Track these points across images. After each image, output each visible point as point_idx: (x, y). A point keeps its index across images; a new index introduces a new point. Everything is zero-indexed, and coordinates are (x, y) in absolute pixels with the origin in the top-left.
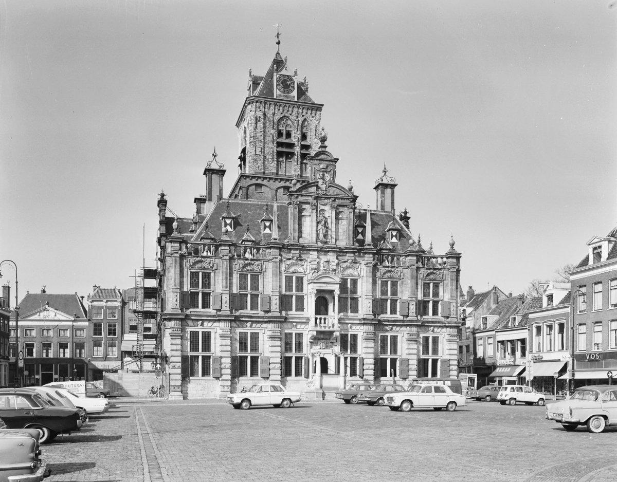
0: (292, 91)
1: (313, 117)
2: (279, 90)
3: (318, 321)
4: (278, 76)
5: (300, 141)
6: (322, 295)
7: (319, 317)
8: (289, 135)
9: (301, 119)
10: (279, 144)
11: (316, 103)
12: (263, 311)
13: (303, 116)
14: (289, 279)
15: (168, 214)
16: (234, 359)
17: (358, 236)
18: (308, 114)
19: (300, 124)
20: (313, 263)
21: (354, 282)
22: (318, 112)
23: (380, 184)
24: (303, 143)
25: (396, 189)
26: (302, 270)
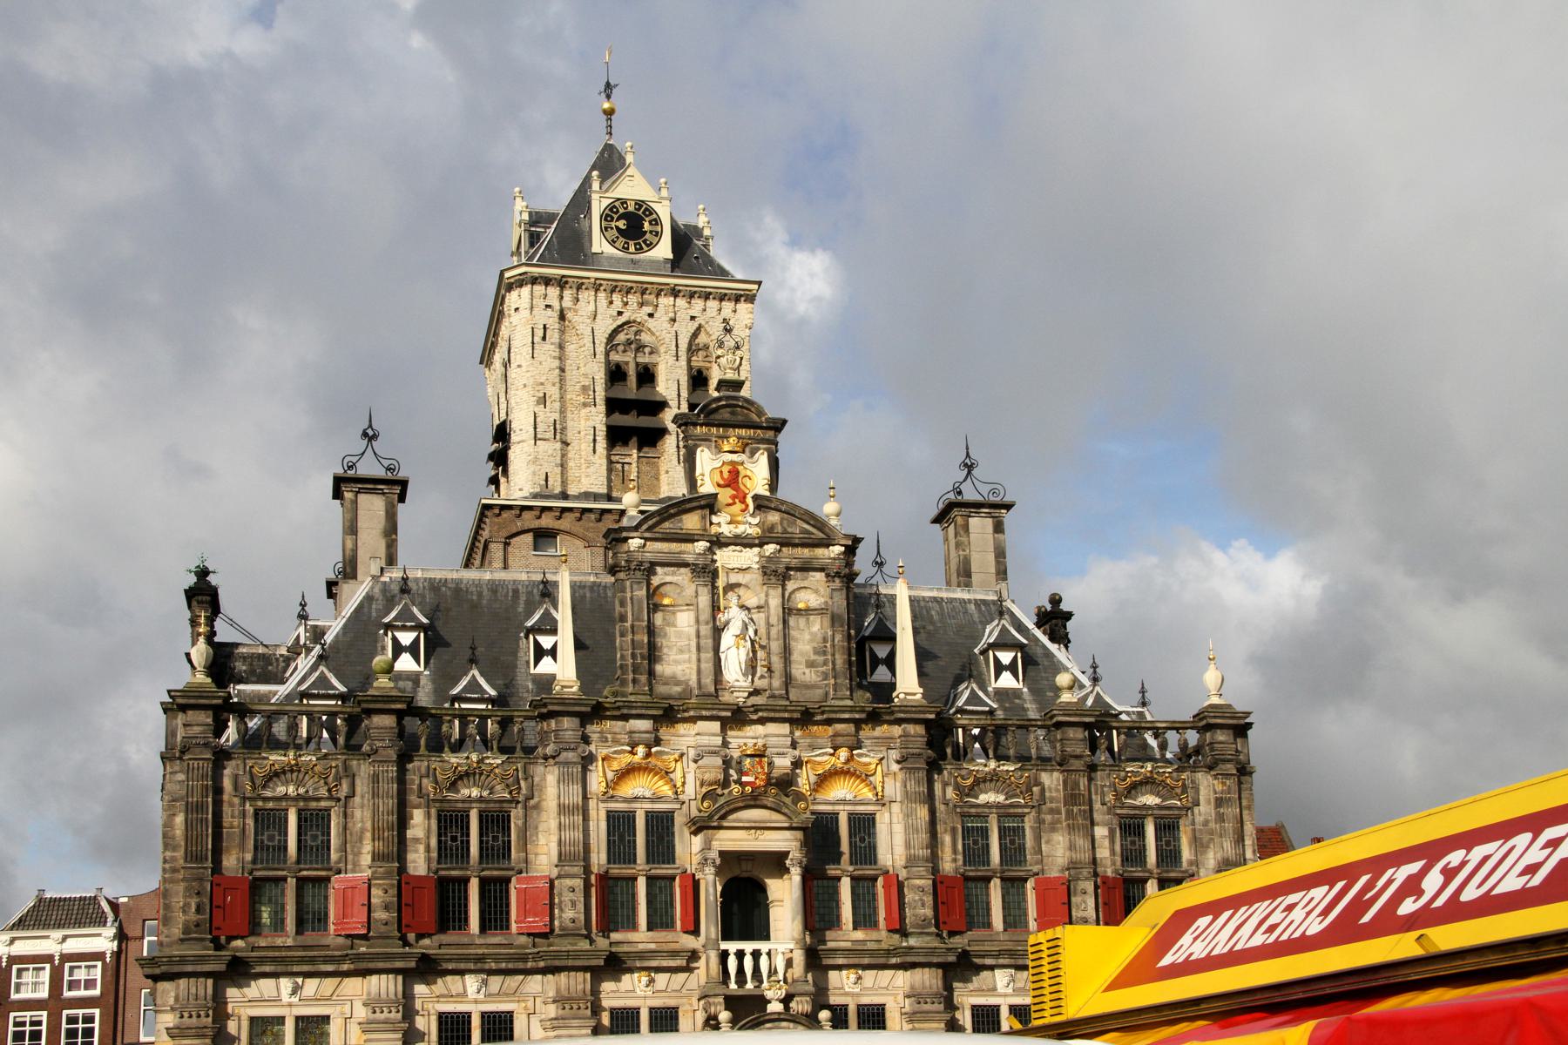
0: (651, 246)
2: (612, 243)
4: (606, 202)
5: (685, 394)
6: (745, 870)
7: (732, 947)
8: (647, 376)
10: (613, 405)
11: (739, 276)
12: (529, 935)
13: (693, 318)
14: (620, 824)
17: (873, 670)
18: (711, 314)
19: (683, 346)
20: (706, 761)
22: (743, 307)
23: (951, 506)
25: (1008, 518)
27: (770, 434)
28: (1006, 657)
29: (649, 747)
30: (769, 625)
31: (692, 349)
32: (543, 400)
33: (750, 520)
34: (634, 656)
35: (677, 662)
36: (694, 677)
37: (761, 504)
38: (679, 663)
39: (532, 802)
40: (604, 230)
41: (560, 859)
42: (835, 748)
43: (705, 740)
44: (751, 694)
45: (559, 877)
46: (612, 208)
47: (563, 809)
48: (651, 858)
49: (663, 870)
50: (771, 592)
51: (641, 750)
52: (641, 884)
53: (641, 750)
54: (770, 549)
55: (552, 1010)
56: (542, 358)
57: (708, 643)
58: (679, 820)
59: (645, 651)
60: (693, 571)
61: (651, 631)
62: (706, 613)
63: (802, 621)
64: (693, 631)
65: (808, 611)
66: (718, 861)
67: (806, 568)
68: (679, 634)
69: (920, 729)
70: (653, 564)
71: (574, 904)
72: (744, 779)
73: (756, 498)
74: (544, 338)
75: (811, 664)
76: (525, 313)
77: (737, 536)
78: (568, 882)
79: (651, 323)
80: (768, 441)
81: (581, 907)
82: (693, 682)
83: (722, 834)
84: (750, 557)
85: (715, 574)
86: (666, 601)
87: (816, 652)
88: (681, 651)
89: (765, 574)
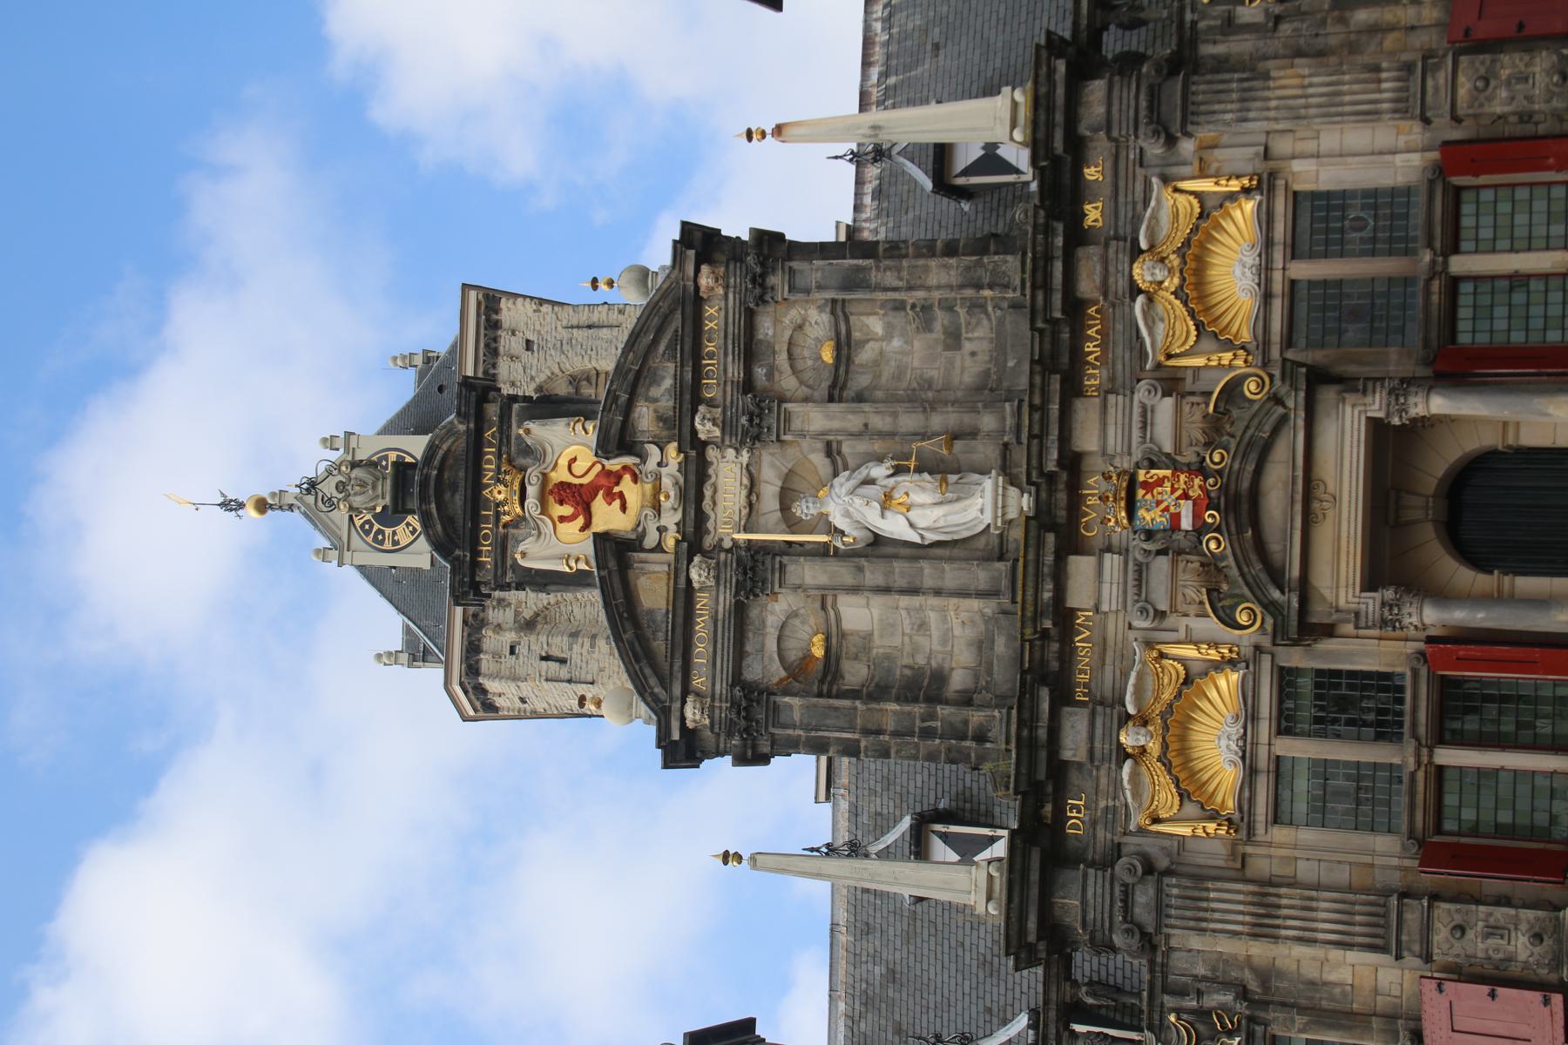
1: (529, 345)
4: (356, 541)
26: (1228, 683)
27: (493, 411)
29: (1126, 718)
30: (865, 432)
33: (652, 464)
34: (927, 733)
35: (946, 637)
36: (975, 604)
37: (619, 440)
38: (950, 632)
39: (1253, 986)
40: (397, 549)
41: (1383, 949)
42: (1135, 290)
43: (1111, 596)
44: (1012, 481)
45: (1428, 958)
47: (1263, 930)
48: (1386, 729)
49: (1419, 706)
50: (796, 424)
51: (1128, 739)
52: (1448, 756)
53: (1128, 739)
56: (594, 667)
57: (900, 572)
59: (918, 709)
60: (752, 592)
61: (877, 692)
62: (843, 573)
63: (865, 355)
64: (878, 601)
65: (845, 346)
66: (1389, 594)
67: (749, 349)
68: (889, 627)
69: (1096, 89)
70: (737, 679)
71: (1493, 931)
72: (1186, 523)
73: (605, 448)
74: (563, 661)
75: (954, 339)
76: (526, 689)
77: (683, 496)
78: (1441, 935)
80: (505, 417)
81: (1501, 913)
82: (989, 607)
83: (1322, 579)
84: (728, 471)
85: (758, 552)
86: (818, 652)
87: (927, 326)
88: (922, 626)
89: (757, 438)
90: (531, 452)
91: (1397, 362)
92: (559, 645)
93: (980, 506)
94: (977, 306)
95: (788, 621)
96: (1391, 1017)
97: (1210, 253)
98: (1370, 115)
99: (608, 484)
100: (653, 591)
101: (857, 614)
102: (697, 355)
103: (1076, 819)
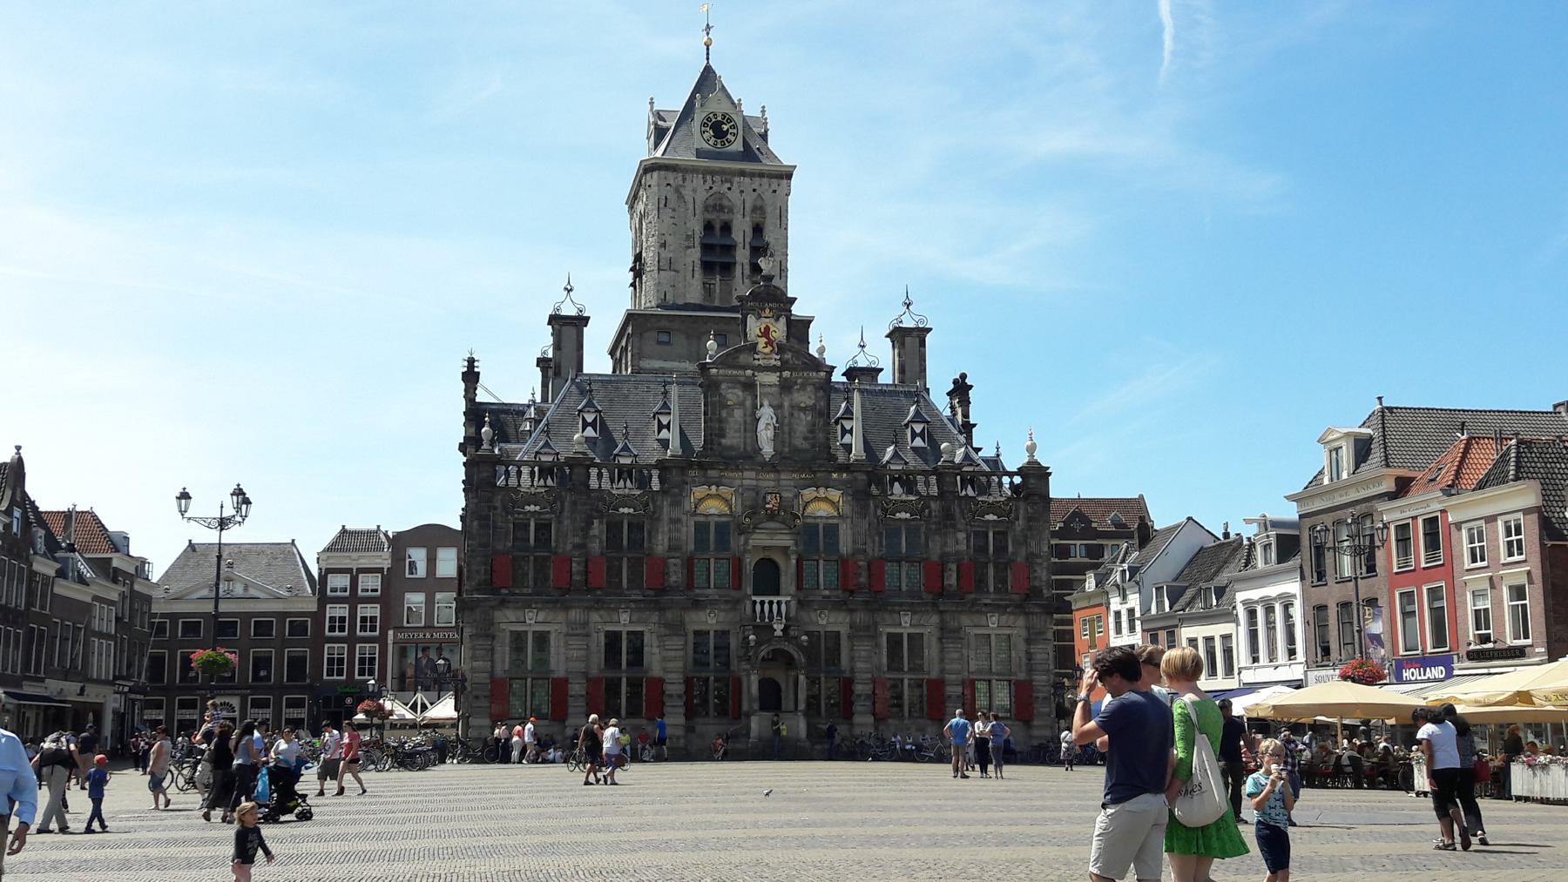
3: (758, 607)
7: (758, 599)
8: (727, 228)
9: (750, 200)
10: (706, 248)
14: (701, 528)
15: (482, 397)
16: (591, 682)
19: (748, 206)
21: (832, 530)
22: (785, 181)
24: (756, 244)
25: (929, 338)
26: (726, 510)
28: (918, 428)
31: (755, 209)
32: (664, 245)
37: (781, 349)
46: (709, 119)
47: (671, 521)
54: (786, 374)
55: (662, 630)
58: (732, 526)
61: (720, 421)
65: (804, 409)
75: (805, 439)
79: (729, 194)
90: (777, 320)
91: (801, 548)
92: (671, 204)
93: (768, 449)
94: (813, 446)
95: (733, 395)
96: (651, 548)
97: (823, 504)
98: (854, 542)
99: (769, 343)
100: (743, 358)
101: (738, 413)
102: (803, 370)
103: (692, 473)
